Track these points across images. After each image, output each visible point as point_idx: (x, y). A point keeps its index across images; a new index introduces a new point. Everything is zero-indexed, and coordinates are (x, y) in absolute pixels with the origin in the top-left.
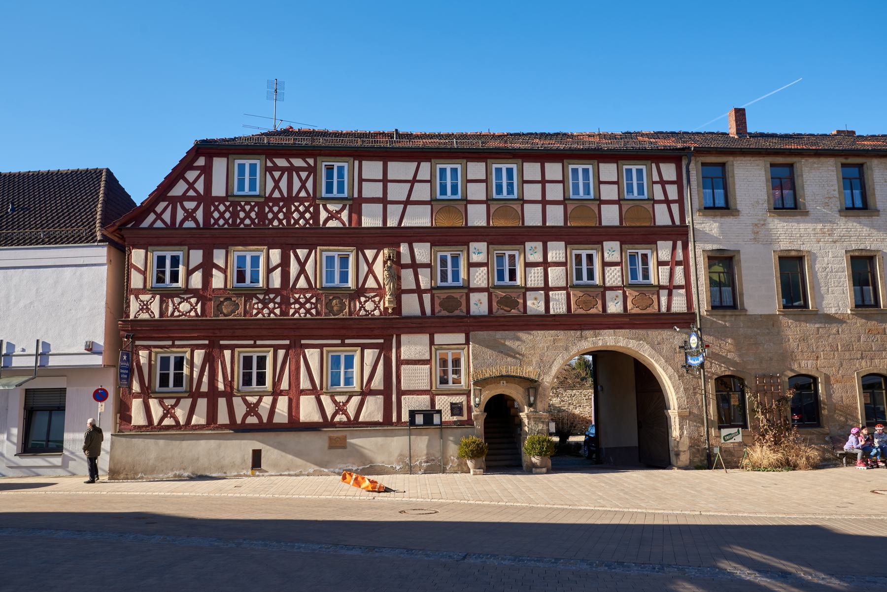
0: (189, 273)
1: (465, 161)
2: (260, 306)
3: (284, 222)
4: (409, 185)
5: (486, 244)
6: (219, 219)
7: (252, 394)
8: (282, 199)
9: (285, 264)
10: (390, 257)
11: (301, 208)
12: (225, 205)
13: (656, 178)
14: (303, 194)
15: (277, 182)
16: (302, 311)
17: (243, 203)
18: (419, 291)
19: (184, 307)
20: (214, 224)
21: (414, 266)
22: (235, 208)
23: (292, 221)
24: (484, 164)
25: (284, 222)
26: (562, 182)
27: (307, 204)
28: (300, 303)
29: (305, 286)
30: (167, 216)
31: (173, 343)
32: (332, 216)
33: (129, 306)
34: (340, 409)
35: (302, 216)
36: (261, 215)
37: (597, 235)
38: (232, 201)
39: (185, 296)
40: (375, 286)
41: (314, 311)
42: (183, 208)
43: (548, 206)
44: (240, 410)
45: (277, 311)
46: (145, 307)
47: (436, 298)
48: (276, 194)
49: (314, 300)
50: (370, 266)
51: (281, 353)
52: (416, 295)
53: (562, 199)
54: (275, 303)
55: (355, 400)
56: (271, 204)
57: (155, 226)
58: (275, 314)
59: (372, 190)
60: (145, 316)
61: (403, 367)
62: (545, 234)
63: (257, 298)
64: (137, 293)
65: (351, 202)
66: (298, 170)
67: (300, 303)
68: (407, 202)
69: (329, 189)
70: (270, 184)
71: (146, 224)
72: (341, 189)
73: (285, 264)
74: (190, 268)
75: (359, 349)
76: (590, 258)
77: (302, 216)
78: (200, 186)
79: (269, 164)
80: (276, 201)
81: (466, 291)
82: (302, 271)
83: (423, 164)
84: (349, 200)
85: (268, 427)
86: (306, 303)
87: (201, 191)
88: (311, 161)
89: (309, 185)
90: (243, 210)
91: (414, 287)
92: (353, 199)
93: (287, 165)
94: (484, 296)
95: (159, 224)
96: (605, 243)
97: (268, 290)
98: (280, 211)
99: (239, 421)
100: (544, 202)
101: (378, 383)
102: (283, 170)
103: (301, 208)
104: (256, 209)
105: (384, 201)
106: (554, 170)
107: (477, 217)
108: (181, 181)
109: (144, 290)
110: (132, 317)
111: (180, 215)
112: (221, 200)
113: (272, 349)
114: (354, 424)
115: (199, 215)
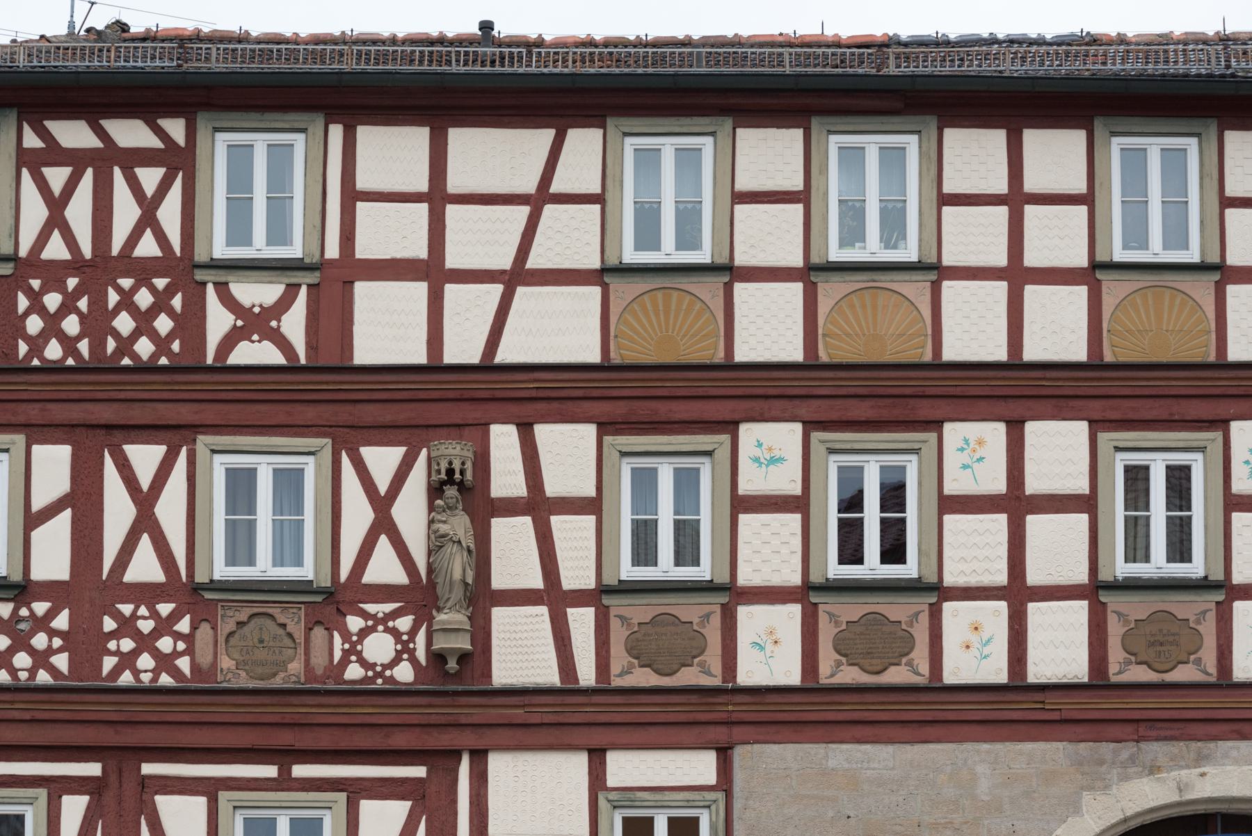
1: (728, 123)
3: (84, 347)
4: (525, 211)
8: (76, 264)
9: (84, 501)
10: (450, 472)
11: (144, 299)
14: (147, 247)
15: (57, 205)
16: (145, 661)
18: (553, 596)
21: (538, 506)
23: (111, 344)
24: (798, 133)
25: (84, 347)
26: (1086, 200)
27: (161, 283)
28: (137, 635)
29: (158, 575)
32: (257, 323)
35: (144, 322)
41: (184, 664)
47: (615, 624)
48: (56, 249)
49: (184, 626)
50: (382, 504)
51: (74, 808)
52: (544, 610)
53: (1083, 262)
56: (36, 284)
58: (53, 671)
62: (1015, 390)
65: (313, 278)
66: (134, 159)
67: (137, 635)
68: (516, 277)
69: (239, 231)
72: (278, 233)
73: (84, 501)
75: (342, 797)
76: (1179, 480)
77: (144, 322)
79: (31, 140)
80: (54, 274)
81: (724, 598)
82: (146, 523)
84: (310, 268)
86: (156, 634)
88: (176, 128)
89: (170, 214)
92: (321, 266)
96: (1235, 425)
98: (67, 307)
100: (1017, 275)
102: (77, 160)
103: (144, 299)
105: (433, 272)
106: (1055, 156)
107: (768, 328)
113: (42, 793)
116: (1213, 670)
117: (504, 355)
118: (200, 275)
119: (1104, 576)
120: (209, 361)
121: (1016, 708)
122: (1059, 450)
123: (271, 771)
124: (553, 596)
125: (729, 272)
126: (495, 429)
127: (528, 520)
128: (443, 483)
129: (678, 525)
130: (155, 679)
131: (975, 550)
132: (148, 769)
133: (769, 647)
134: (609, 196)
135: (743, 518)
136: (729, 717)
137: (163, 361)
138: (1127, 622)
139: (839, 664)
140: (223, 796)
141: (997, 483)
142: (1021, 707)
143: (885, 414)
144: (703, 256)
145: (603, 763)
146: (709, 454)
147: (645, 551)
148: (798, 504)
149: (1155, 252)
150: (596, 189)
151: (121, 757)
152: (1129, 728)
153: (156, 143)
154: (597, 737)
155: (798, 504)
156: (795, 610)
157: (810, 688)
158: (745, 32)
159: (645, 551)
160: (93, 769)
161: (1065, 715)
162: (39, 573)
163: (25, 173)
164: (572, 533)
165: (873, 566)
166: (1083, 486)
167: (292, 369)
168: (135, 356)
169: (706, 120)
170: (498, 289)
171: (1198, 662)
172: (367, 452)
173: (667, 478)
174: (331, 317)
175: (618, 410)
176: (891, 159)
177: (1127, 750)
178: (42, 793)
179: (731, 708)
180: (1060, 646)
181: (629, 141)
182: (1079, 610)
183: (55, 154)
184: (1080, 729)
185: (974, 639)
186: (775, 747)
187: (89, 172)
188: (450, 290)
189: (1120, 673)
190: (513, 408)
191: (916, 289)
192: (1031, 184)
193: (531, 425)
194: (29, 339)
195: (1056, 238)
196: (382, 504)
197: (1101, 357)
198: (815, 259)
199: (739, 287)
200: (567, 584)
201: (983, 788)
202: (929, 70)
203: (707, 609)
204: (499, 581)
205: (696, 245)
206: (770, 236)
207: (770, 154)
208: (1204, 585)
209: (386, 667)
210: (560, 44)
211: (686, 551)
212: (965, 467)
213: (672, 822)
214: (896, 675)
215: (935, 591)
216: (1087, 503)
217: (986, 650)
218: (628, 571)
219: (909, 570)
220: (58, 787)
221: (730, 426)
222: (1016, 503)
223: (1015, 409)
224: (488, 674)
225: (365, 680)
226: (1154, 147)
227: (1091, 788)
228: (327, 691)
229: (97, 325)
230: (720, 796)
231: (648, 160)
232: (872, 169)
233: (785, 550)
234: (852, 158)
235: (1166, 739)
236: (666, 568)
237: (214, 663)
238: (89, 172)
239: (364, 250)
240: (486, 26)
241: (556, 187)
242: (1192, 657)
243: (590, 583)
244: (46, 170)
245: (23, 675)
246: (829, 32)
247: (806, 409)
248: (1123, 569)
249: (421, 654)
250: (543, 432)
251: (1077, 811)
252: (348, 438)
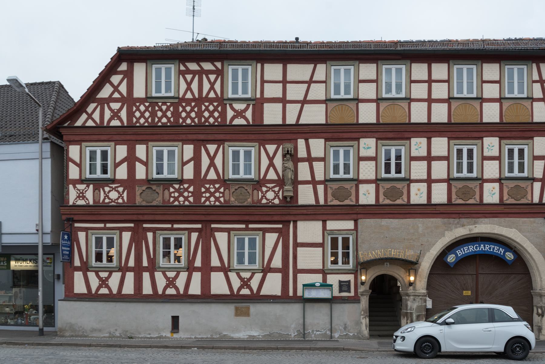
0: (117, 165)
1: (357, 62)
2: (176, 194)
3: (196, 120)
5: (375, 139)
6: (140, 118)
7: (171, 269)
8: (194, 99)
9: (197, 159)
10: (288, 151)
11: (211, 108)
12: (145, 106)
13: (536, 77)
14: (212, 95)
15: (189, 84)
16: (212, 199)
17: (160, 104)
18: (314, 182)
19: (114, 195)
20: (136, 122)
21: (310, 160)
22: (153, 108)
23: (203, 120)
25: (196, 120)
26: (448, 81)
27: (215, 104)
28: (210, 192)
30: (96, 116)
31: (105, 225)
33: (68, 194)
34: (245, 283)
35: (211, 114)
36: (177, 114)
37: (477, 130)
38: (151, 102)
39: (114, 186)
40: (275, 177)
41: (222, 199)
42: (110, 108)
43: (433, 104)
44: (161, 282)
45: (191, 199)
46: (81, 195)
47: (329, 189)
48: (189, 96)
49: (222, 190)
51: (194, 236)
52: (311, 186)
53: (447, 97)
54: (189, 192)
55: (258, 277)
56: (184, 104)
57: (87, 125)
59: (273, 91)
60: (81, 202)
61: (299, 249)
62: (429, 130)
63: (174, 188)
64: (74, 182)
65: (254, 102)
66: (208, 73)
67: (210, 192)
68: (304, 102)
69: (235, 91)
70: (183, 86)
71: (79, 123)
72: (245, 91)
73: (197, 159)
74: (117, 161)
75: (261, 232)
76: (470, 152)
77: (211, 114)
78: (123, 88)
79: (182, 68)
80: (188, 102)
82: (212, 164)
83: (319, 66)
85: (185, 298)
86: (215, 192)
87: (125, 94)
88: (219, 64)
89: (217, 87)
90: (161, 110)
91: (309, 179)
92: (255, 99)
93: (198, 68)
94: (372, 187)
95: (90, 123)
96: (484, 139)
97: (181, 181)
98: (192, 110)
99: (160, 292)
100: (430, 101)
101: (277, 262)
102: (194, 73)
103: (211, 108)
104: (172, 109)
105: (283, 101)
106: (440, 70)
107: (367, 114)
108: (108, 85)
109: (81, 181)
110: (71, 203)
111: (108, 114)
112: (142, 101)
113: (186, 232)
114: (257, 298)
115: (123, 114)
116: (478, 201)
117: (301, 122)
118: (225, 102)
119: (451, 177)
120: (105, 124)
121: (429, 210)
122: (440, 145)
123: (243, 226)
124: (314, 182)
125: (357, 100)
126: (299, 140)
127: (307, 163)
128: (286, 154)
129: (345, 164)
130: (215, 203)
131: (418, 170)
132: (213, 226)
133: (367, 195)
134: (327, 81)
135: (361, 162)
136: (357, 212)
137: (216, 124)
138: (457, 188)
139: (384, 199)
140: (232, 232)
141: (425, 154)
142: (430, 210)
143: (396, 136)
144: (351, 96)
145: (326, 224)
146: (352, 146)
147: (336, 171)
148: (374, 159)
149: (465, 94)
150: (324, 79)
151: (206, 223)
152: (457, 215)
153: (214, 68)
154: (324, 217)
155: (374, 159)
156: (374, 185)
157: (377, 205)
158: (362, 40)
159: (336, 171)
160: (199, 226)
161: (441, 212)
162: (118, 177)
163: (181, 76)
164: (319, 167)
165: (393, 174)
166: (446, 154)
167: (123, 127)
168: (209, 122)
169: (352, 62)
170: (300, 105)
171: (475, 198)
172: (267, 146)
173: (342, 152)
174: (258, 112)
175: (329, 135)
176: (399, 71)
177: (457, 221)
178: (186, 232)
179: (358, 210)
180: (440, 194)
181: (333, 67)
182: (445, 186)
183: (188, 71)
184: (444, 215)
185: (418, 192)
186: (369, 220)
187: (197, 76)
188: (288, 105)
190: (304, 135)
191: (404, 104)
192: (434, 77)
193: (308, 139)
194: (182, 118)
195: (440, 91)
196: (271, 159)
197: (451, 121)
198: (379, 97)
199: (360, 104)
200: (317, 179)
201: (420, 230)
202: (408, 49)
203: (351, 185)
204: (300, 178)
205: (349, 94)
206: (368, 91)
207: (368, 70)
208: (476, 179)
209: (272, 200)
210: (315, 43)
211: (347, 171)
212: (416, 149)
213: (343, 238)
214: (399, 202)
215: (409, 181)
216: (447, 158)
217: (421, 195)
218: (332, 176)
219: (402, 175)
220: (122, 230)
221: (358, 139)
222: (429, 158)
223: (429, 135)
224: (297, 202)
225: (267, 203)
226: (465, 68)
227: (447, 230)
228: (167, 206)
229: (153, 114)
230: (355, 232)
231: (337, 72)
232: (393, 73)
233: (371, 170)
234: (389, 71)
235: (466, 218)
236: (341, 175)
237: (229, 200)
238: (197, 76)
239: (267, 95)
240: (297, 39)
241: (314, 79)
243: (323, 179)
244: (186, 76)
245: (182, 203)
246: (383, 40)
247: (377, 135)
248: (456, 175)
249: (281, 197)
250: (311, 141)
251: (444, 236)
252: (263, 143)
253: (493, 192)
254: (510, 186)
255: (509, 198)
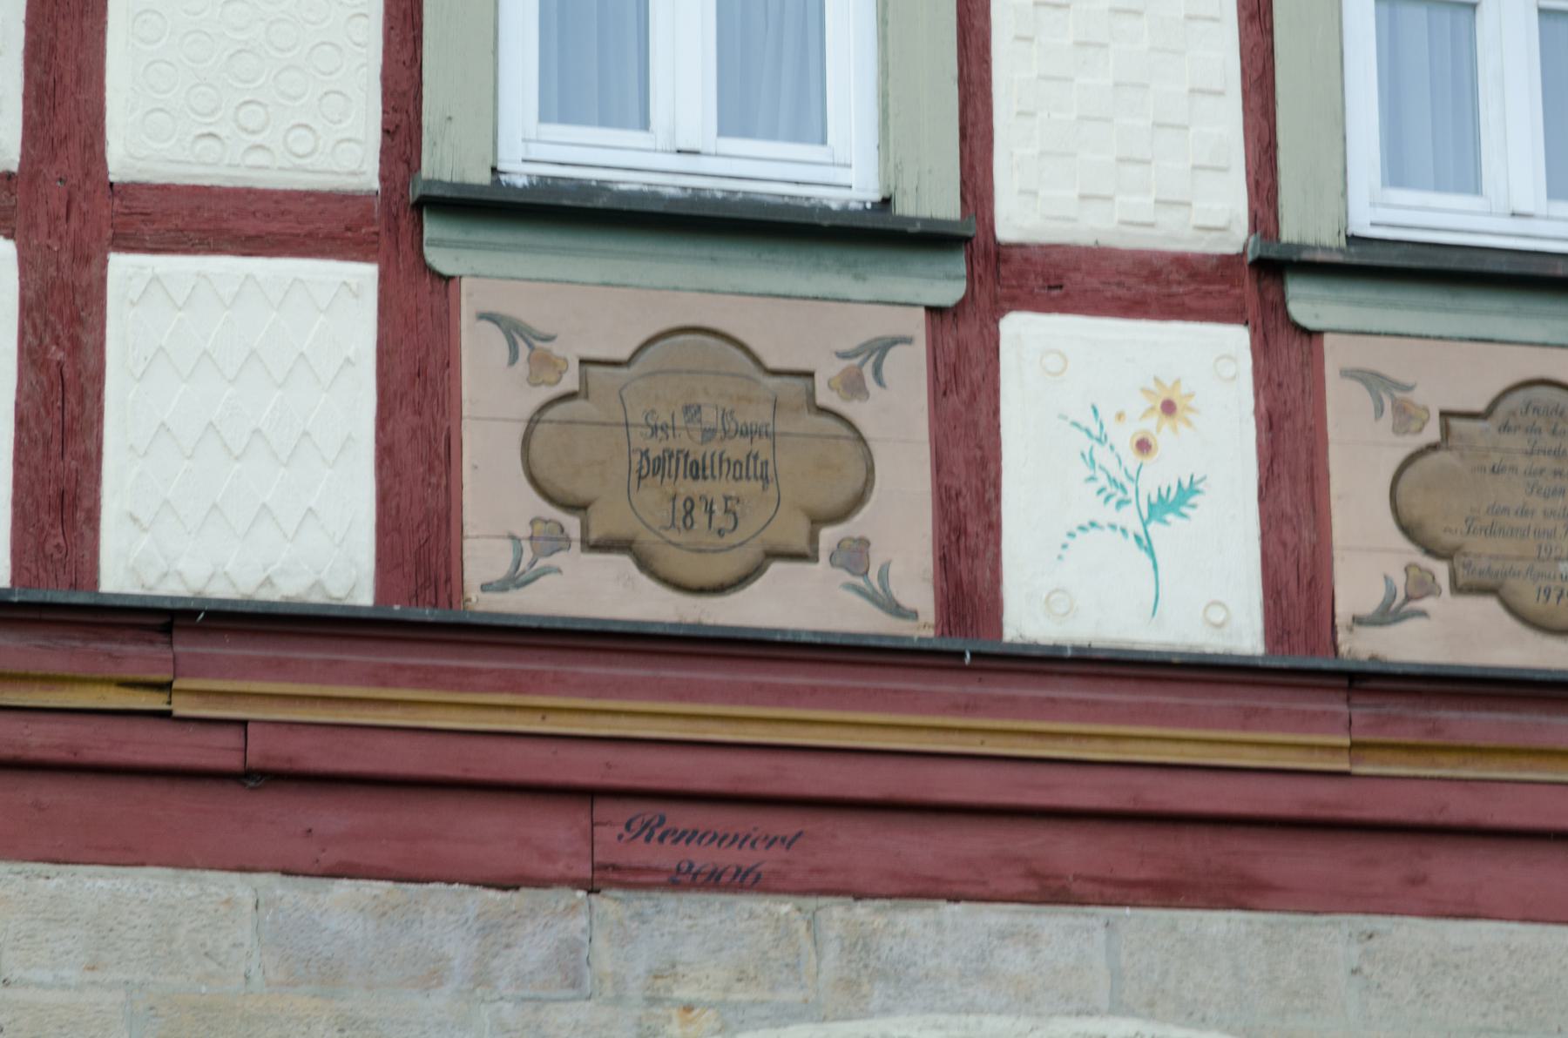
116: (918, 592)
171: (855, 556)
182: (338, 299)
189: (514, 581)
242: (829, 536)
253: (1158, 475)
254: (1433, 395)
255: (1422, 586)
